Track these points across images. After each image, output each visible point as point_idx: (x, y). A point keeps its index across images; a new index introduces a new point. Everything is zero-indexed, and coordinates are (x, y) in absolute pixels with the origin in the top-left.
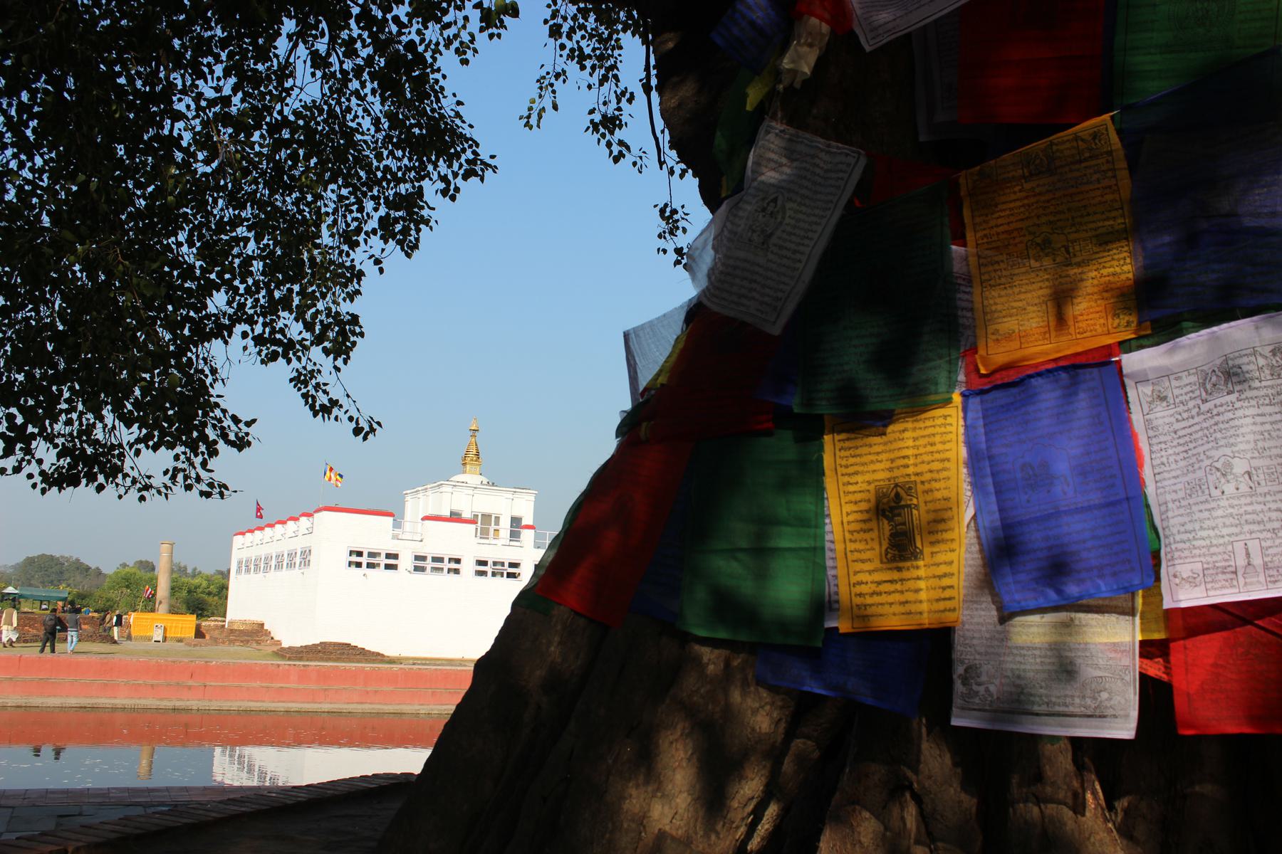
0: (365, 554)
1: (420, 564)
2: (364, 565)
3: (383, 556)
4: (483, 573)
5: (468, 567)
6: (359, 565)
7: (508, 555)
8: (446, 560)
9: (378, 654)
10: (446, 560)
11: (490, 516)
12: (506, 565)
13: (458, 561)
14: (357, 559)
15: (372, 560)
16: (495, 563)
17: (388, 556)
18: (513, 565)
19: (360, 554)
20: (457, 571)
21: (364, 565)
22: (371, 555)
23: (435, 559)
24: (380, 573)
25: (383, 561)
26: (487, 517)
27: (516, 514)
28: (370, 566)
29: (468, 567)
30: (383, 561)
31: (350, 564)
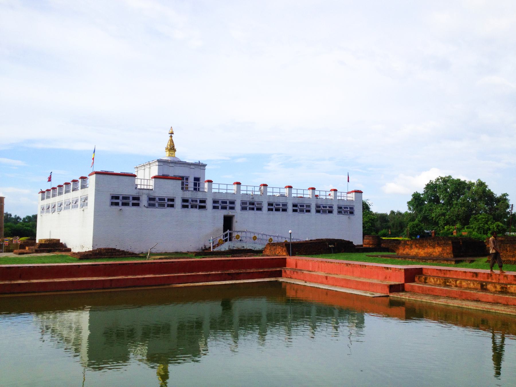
0: (121, 198)
1: (152, 202)
2: (120, 204)
3: (131, 199)
4: (187, 207)
5: (178, 203)
6: (117, 204)
7: (199, 196)
8: (166, 200)
10: (166, 200)
12: (198, 201)
13: (172, 200)
15: (125, 201)
16: (192, 201)
17: (134, 198)
18: (201, 201)
19: (117, 198)
20: (172, 206)
21: (120, 204)
22: (125, 198)
23: (160, 199)
24: (129, 210)
25: (131, 201)
26: (181, 178)
27: (197, 176)
28: (124, 204)
29: (178, 203)
30: (131, 201)
31: (112, 204)
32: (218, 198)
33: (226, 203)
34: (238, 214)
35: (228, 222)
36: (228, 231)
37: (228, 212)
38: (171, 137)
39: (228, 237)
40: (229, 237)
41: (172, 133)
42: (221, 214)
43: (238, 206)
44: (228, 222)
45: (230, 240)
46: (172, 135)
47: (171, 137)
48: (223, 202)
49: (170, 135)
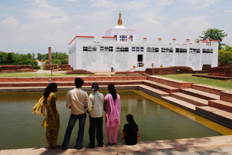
9: (89, 72)
11: (124, 36)
14: (85, 49)
26: (123, 37)
32: (134, 46)
33: (139, 48)
34: (145, 54)
35: (140, 58)
36: (139, 62)
37: (140, 53)
38: (120, 16)
39: (139, 65)
40: (141, 65)
41: (120, 15)
42: (136, 54)
43: (145, 50)
44: (140, 58)
45: (140, 66)
46: (121, 15)
47: (120, 16)
48: (137, 48)
49: (119, 15)
